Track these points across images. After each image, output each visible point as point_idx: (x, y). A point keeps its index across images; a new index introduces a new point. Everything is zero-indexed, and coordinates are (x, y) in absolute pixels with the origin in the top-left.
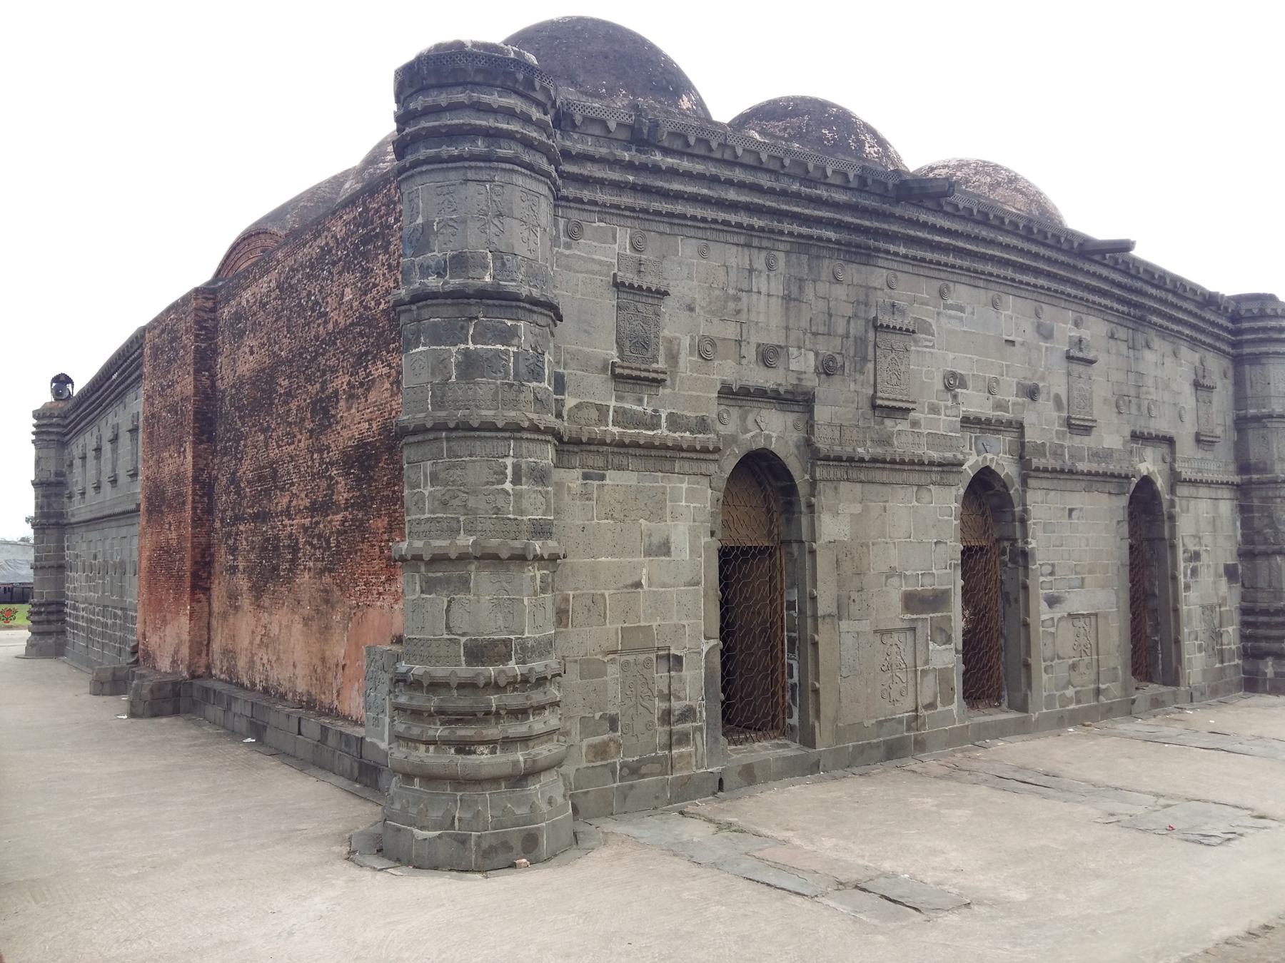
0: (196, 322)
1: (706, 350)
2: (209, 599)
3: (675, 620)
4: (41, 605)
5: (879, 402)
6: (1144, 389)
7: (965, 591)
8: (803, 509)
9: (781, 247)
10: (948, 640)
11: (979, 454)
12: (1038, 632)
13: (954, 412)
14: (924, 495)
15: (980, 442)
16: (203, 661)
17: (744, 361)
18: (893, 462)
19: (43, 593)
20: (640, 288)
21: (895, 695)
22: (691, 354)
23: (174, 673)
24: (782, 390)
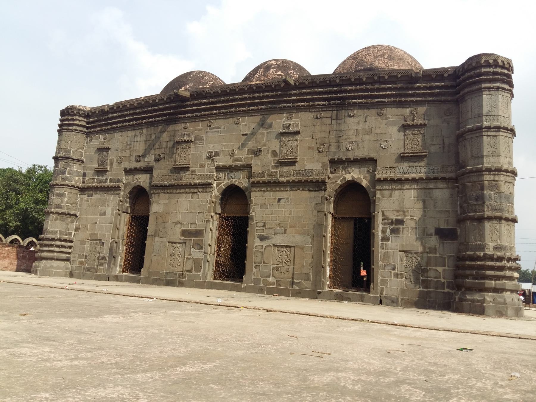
12: (252, 250)
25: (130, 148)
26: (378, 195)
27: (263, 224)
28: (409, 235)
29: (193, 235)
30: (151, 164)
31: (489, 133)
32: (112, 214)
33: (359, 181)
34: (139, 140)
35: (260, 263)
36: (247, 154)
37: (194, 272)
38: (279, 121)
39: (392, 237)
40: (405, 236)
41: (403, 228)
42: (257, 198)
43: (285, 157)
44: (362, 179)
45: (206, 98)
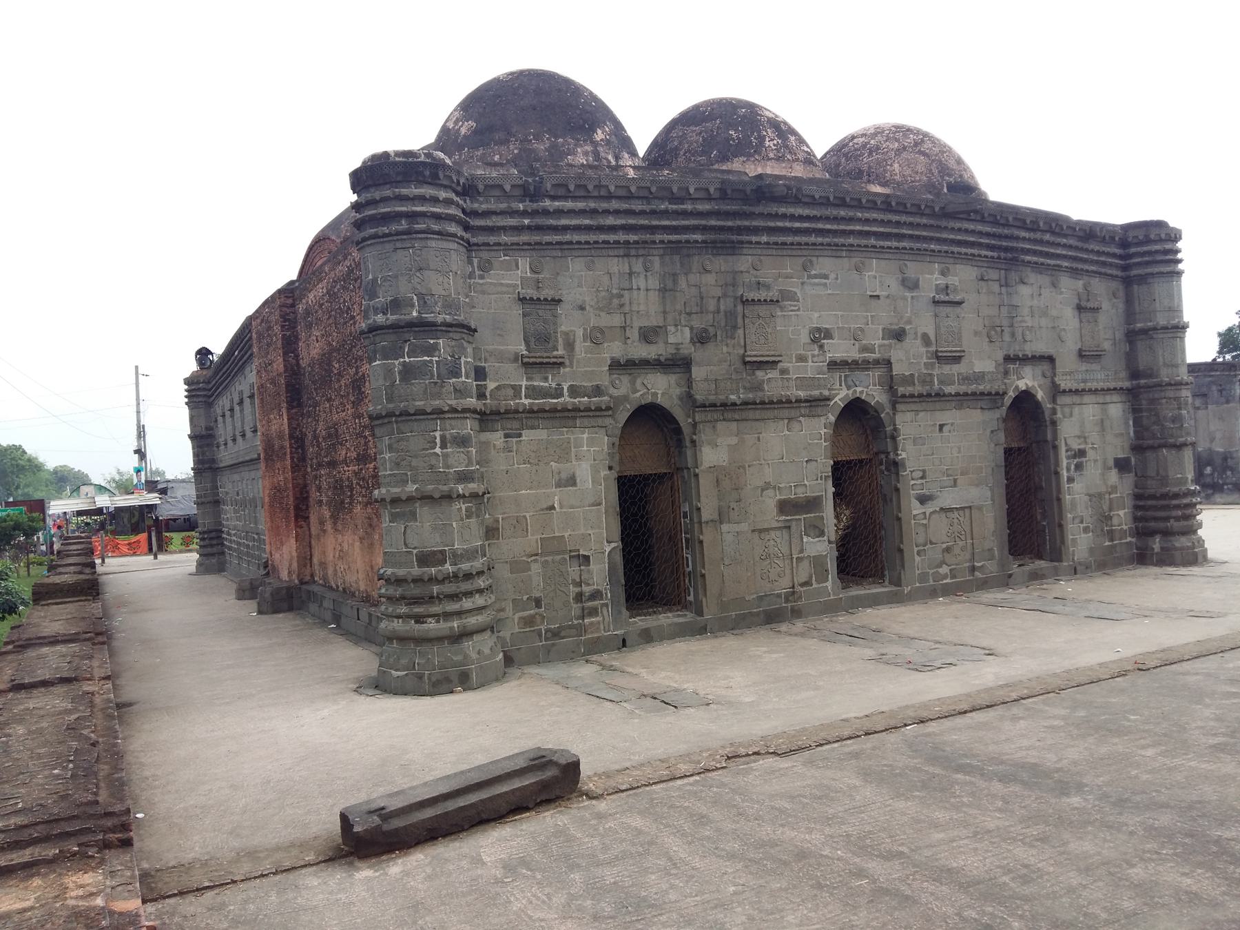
0: (281, 316)
1: (596, 337)
2: (309, 525)
3: (582, 531)
4: (204, 533)
5: (748, 359)
6: (1019, 319)
7: (836, 495)
8: (688, 444)
9: (656, 252)
10: (822, 534)
11: (849, 388)
13: (821, 358)
14: (795, 425)
15: (849, 379)
16: (308, 572)
17: (629, 341)
18: (763, 403)
19: (205, 523)
20: (539, 299)
21: (772, 577)
22: (585, 341)
23: (290, 581)
24: (662, 359)
27: (921, 474)
43: (945, 349)
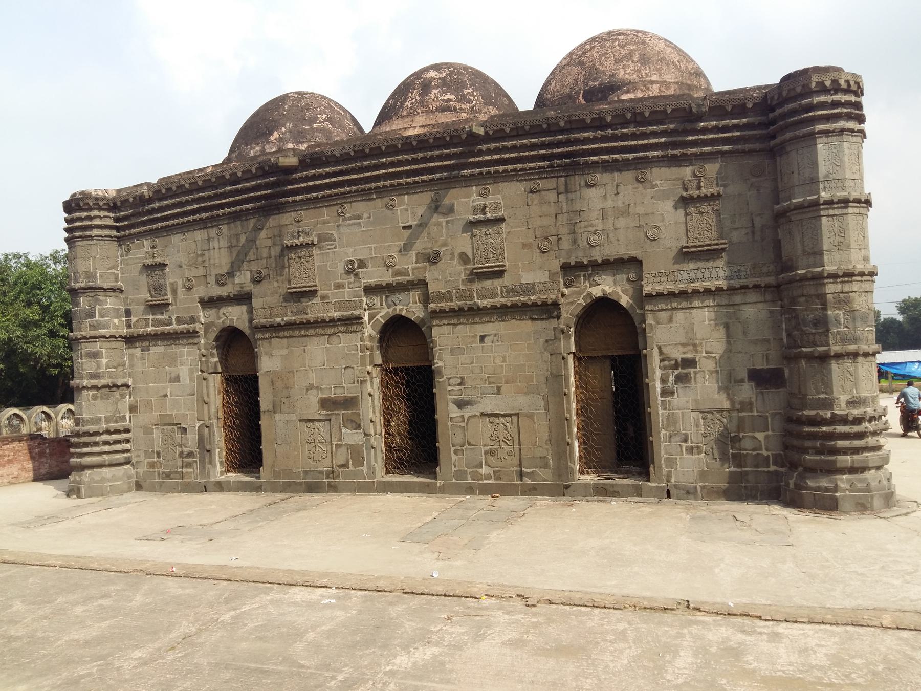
12: (446, 425)
13: (357, 284)
25: (204, 261)
26: (650, 320)
27: (459, 381)
28: (707, 383)
29: (340, 406)
30: (247, 289)
31: (831, 212)
32: (191, 379)
33: (614, 298)
34: (216, 246)
35: (463, 445)
36: (416, 262)
37: (351, 468)
38: (466, 201)
39: (679, 389)
40: (699, 386)
41: (695, 373)
42: (443, 336)
43: (482, 265)
44: (620, 293)
45: (327, 164)
